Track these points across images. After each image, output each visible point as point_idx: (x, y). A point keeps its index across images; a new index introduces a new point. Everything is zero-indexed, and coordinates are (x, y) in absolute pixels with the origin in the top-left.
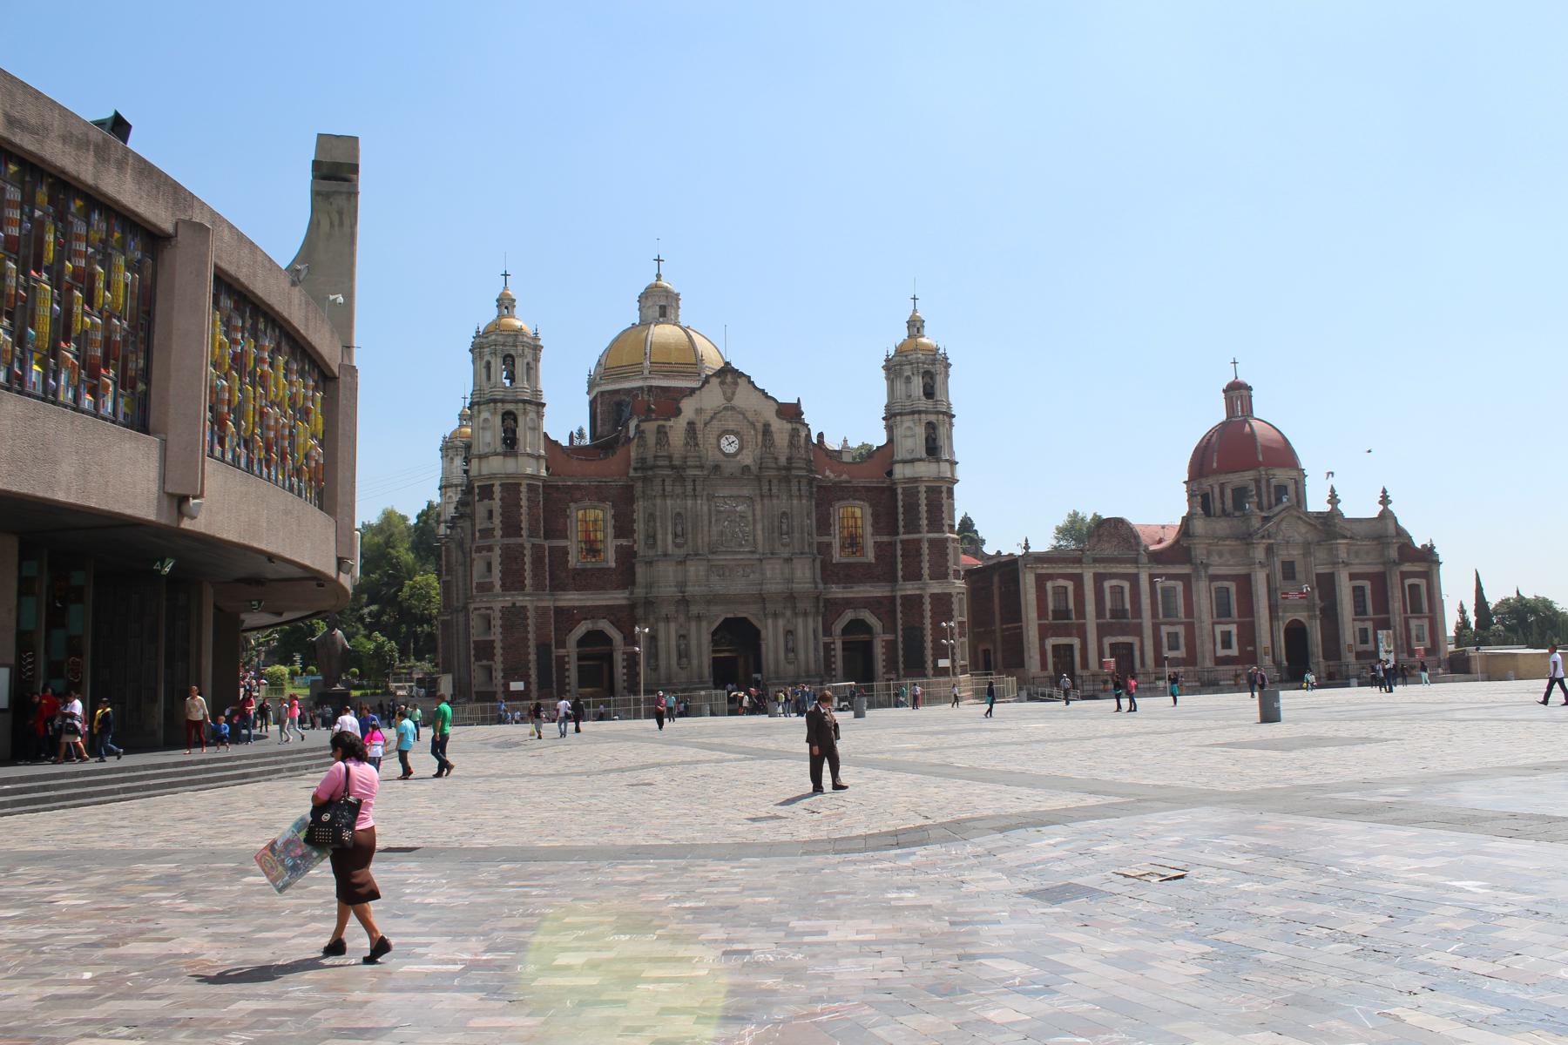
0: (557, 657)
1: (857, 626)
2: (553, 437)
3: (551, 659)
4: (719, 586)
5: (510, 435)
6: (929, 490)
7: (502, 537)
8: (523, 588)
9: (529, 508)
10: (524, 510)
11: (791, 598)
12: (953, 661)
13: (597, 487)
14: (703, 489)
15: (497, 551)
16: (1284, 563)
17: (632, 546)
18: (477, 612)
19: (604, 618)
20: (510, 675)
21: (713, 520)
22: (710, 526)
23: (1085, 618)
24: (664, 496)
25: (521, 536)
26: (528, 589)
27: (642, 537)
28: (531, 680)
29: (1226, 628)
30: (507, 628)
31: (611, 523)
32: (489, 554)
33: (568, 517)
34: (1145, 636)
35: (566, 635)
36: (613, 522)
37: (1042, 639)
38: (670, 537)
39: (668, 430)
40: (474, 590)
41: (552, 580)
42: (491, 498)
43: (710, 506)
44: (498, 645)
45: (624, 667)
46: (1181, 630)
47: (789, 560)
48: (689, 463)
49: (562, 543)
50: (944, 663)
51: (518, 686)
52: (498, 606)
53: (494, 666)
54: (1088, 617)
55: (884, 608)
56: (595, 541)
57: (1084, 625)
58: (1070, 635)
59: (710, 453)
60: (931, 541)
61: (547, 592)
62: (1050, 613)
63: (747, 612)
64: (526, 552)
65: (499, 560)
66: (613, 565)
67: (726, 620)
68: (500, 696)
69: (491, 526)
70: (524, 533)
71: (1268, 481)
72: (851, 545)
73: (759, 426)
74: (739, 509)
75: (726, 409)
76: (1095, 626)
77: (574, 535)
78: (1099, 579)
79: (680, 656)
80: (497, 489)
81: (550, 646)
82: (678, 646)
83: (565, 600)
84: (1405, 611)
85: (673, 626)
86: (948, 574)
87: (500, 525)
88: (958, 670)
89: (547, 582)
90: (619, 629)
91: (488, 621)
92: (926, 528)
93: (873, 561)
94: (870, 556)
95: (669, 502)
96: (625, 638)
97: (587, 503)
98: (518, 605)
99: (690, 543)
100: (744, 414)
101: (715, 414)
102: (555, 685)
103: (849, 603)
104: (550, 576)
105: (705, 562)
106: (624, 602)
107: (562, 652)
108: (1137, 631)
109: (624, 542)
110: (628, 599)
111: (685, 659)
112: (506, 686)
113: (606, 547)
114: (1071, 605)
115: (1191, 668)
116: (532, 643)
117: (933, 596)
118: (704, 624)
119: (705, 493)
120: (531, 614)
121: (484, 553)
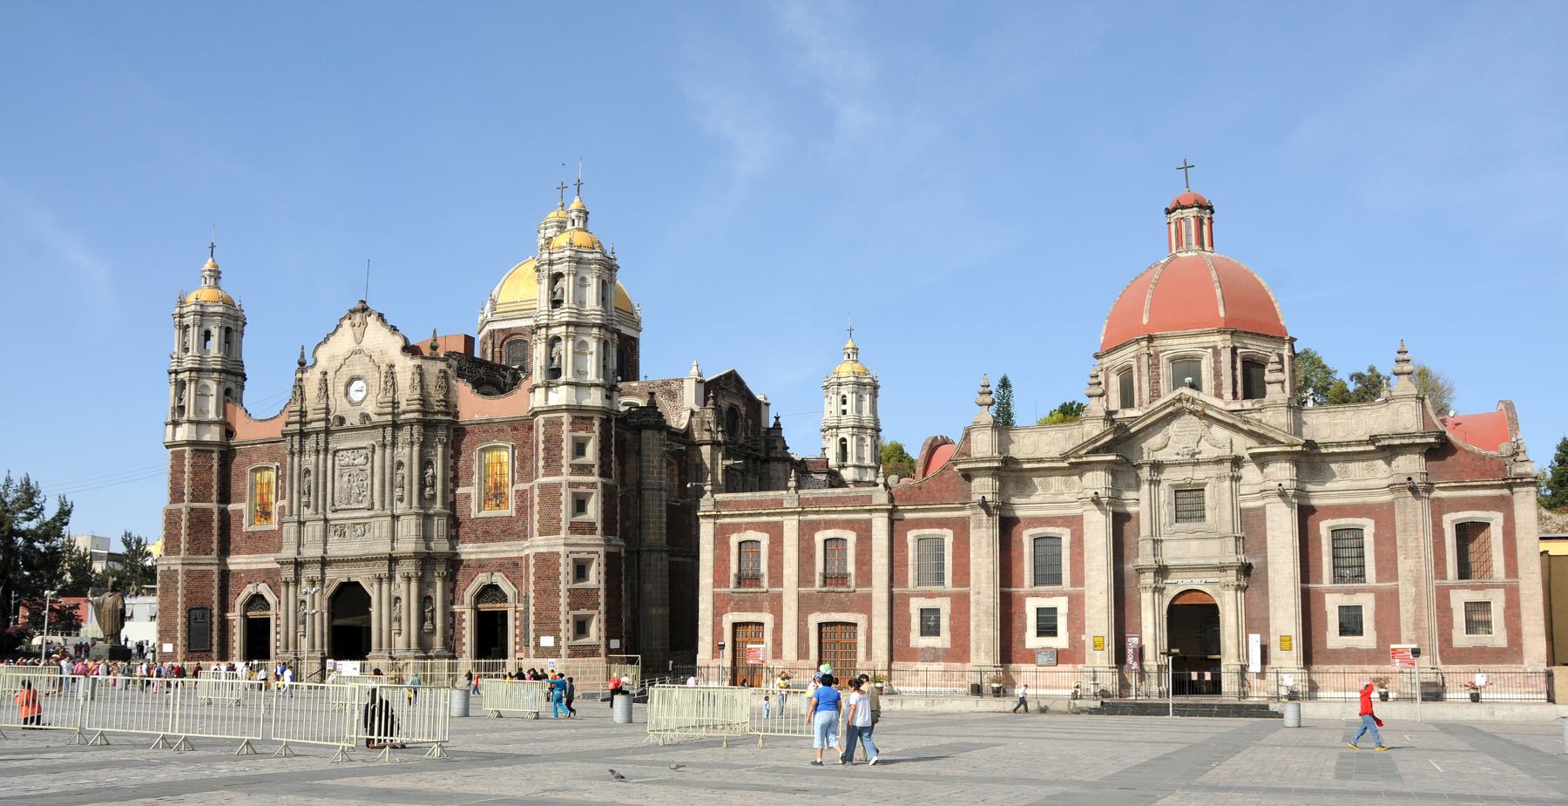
1: (490, 591)
4: (336, 549)
5: (182, 404)
6: (547, 423)
9: (195, 473)
11: (393, 560)
12: (558, 639)
16: (1178, 490)
19: (264, 582)
23: (782, 586)
25: (184, 501)
28: (179, 642)
29: (1046, 603)
34: (874, 613)
37: (717, 615)
39: (304, 383)
46: (944, 606)
47: (395, 518)
50: (547, 641)
51: (168, 648)
54: (785, 583)
55: (513, 567)
57: (780, 596)
58: (760, 610)
60: (542, 487)
62: (732, 579)
63: (362, 576)
70: (186, 498)
71: (1154, 358)
72: (495, 496)
73: (384, 368)
74: (356, 462)
75: (354, 353)
76: (795, 597)
78: (806, 531)
84: (1441, 572)
86: (560, 528)
88: (563, 652)
89: (215, 546)
90: (275, 593)
92: (541, 471)
93: (514, 515)
94: (509, 510)
100: (371, 357)
101: (345, 359)
103: (481, 565)
108: (865, 605)
114: (764, 568)
115: (959, 664)
117: (537, 556)
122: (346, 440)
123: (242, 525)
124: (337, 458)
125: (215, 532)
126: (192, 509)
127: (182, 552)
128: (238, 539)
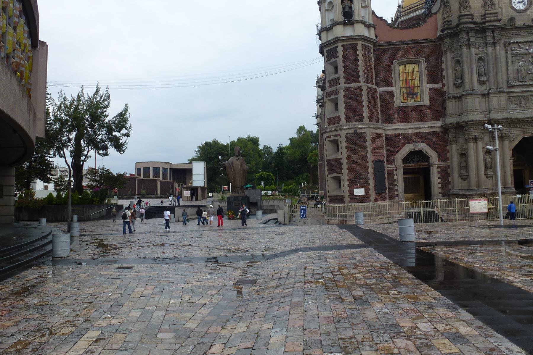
0: (388, 171)
2: (379, 15)
3: (384, 173)
4: (518, 114)
5: (347, 9)
7: (345, 83)
8: (361, 119)
9: (364, 62)
10: (361, 63)
13: (413, 47)
14: (501, 38)
15: (342, 93)
17: (442, 89)
18: (329, 139)
19: (422, 142)
20: (354, 183)
21: (510, 61)
22: (507, 66)
24: (469, 45)
25: (359, 82)
26: (366, 120)
27: (451, 79)
28: (370, 187)
30: (351, 149)
31: (425, 72)
32: (336, 96)
33: (392, 70)
35: (395, 155)
36: (426, 72)
38: (475, 76)
40: (326, 124)
41: (382, 116)
42: (336, 56)
43: (506, 50)
44: (345, 161)
45: (439, 178)
48: (488, 19)
49: (389, 89)
51: (359, 191)
52: (343, 133)
53: (342, 178)
56: (413, 87)
59: (504, 10)
61: (380, 123)
64: (363, 93)
65: (343, 100)
66: (428, 103)
67: (524, 139)
68: (347, 199)
69: (336, 76)
70: (361, 79)
77: (397, 83)
79: (486, 168)
80: (340, 49)
81: (383, 162)
82: (485, 161)
83: (392, 129)
85: (480, 145)
87: (343, 75)
89: (380, 116)
91: (336, 143)
95: (473, 50)
96: (439, 156)
97: (406, 59)
98: (358, 131)
99: (492, 79)
102: (387, 190)
104: (382, 111)
105: (506, 95)
106: (438, 130)
107: (392, 167)
109: (436, 86)
110: (441, 127)
111: (491, 170)
112: (351, 191)
113: (422, 91)
116: (370, 160)
118: (506, 142)
119: (503, 41)
120: (369, 138)
121: (333, 97)
122: (517, 36)
123: (394, 102)
124: (509, 49)
125: (379, 105)
126: (368, 87)
127: (365, 119)
128: (390, 112)
